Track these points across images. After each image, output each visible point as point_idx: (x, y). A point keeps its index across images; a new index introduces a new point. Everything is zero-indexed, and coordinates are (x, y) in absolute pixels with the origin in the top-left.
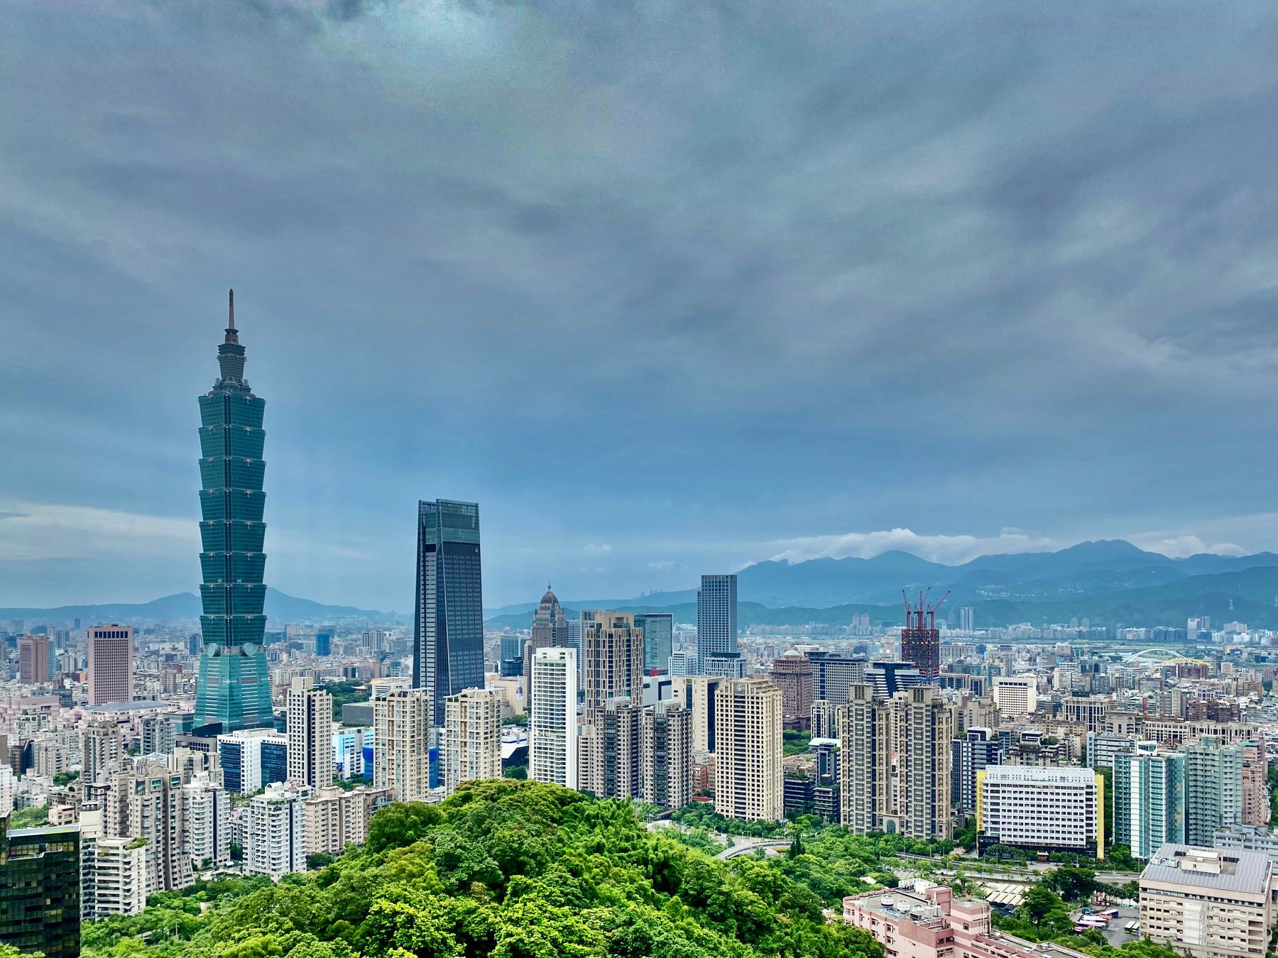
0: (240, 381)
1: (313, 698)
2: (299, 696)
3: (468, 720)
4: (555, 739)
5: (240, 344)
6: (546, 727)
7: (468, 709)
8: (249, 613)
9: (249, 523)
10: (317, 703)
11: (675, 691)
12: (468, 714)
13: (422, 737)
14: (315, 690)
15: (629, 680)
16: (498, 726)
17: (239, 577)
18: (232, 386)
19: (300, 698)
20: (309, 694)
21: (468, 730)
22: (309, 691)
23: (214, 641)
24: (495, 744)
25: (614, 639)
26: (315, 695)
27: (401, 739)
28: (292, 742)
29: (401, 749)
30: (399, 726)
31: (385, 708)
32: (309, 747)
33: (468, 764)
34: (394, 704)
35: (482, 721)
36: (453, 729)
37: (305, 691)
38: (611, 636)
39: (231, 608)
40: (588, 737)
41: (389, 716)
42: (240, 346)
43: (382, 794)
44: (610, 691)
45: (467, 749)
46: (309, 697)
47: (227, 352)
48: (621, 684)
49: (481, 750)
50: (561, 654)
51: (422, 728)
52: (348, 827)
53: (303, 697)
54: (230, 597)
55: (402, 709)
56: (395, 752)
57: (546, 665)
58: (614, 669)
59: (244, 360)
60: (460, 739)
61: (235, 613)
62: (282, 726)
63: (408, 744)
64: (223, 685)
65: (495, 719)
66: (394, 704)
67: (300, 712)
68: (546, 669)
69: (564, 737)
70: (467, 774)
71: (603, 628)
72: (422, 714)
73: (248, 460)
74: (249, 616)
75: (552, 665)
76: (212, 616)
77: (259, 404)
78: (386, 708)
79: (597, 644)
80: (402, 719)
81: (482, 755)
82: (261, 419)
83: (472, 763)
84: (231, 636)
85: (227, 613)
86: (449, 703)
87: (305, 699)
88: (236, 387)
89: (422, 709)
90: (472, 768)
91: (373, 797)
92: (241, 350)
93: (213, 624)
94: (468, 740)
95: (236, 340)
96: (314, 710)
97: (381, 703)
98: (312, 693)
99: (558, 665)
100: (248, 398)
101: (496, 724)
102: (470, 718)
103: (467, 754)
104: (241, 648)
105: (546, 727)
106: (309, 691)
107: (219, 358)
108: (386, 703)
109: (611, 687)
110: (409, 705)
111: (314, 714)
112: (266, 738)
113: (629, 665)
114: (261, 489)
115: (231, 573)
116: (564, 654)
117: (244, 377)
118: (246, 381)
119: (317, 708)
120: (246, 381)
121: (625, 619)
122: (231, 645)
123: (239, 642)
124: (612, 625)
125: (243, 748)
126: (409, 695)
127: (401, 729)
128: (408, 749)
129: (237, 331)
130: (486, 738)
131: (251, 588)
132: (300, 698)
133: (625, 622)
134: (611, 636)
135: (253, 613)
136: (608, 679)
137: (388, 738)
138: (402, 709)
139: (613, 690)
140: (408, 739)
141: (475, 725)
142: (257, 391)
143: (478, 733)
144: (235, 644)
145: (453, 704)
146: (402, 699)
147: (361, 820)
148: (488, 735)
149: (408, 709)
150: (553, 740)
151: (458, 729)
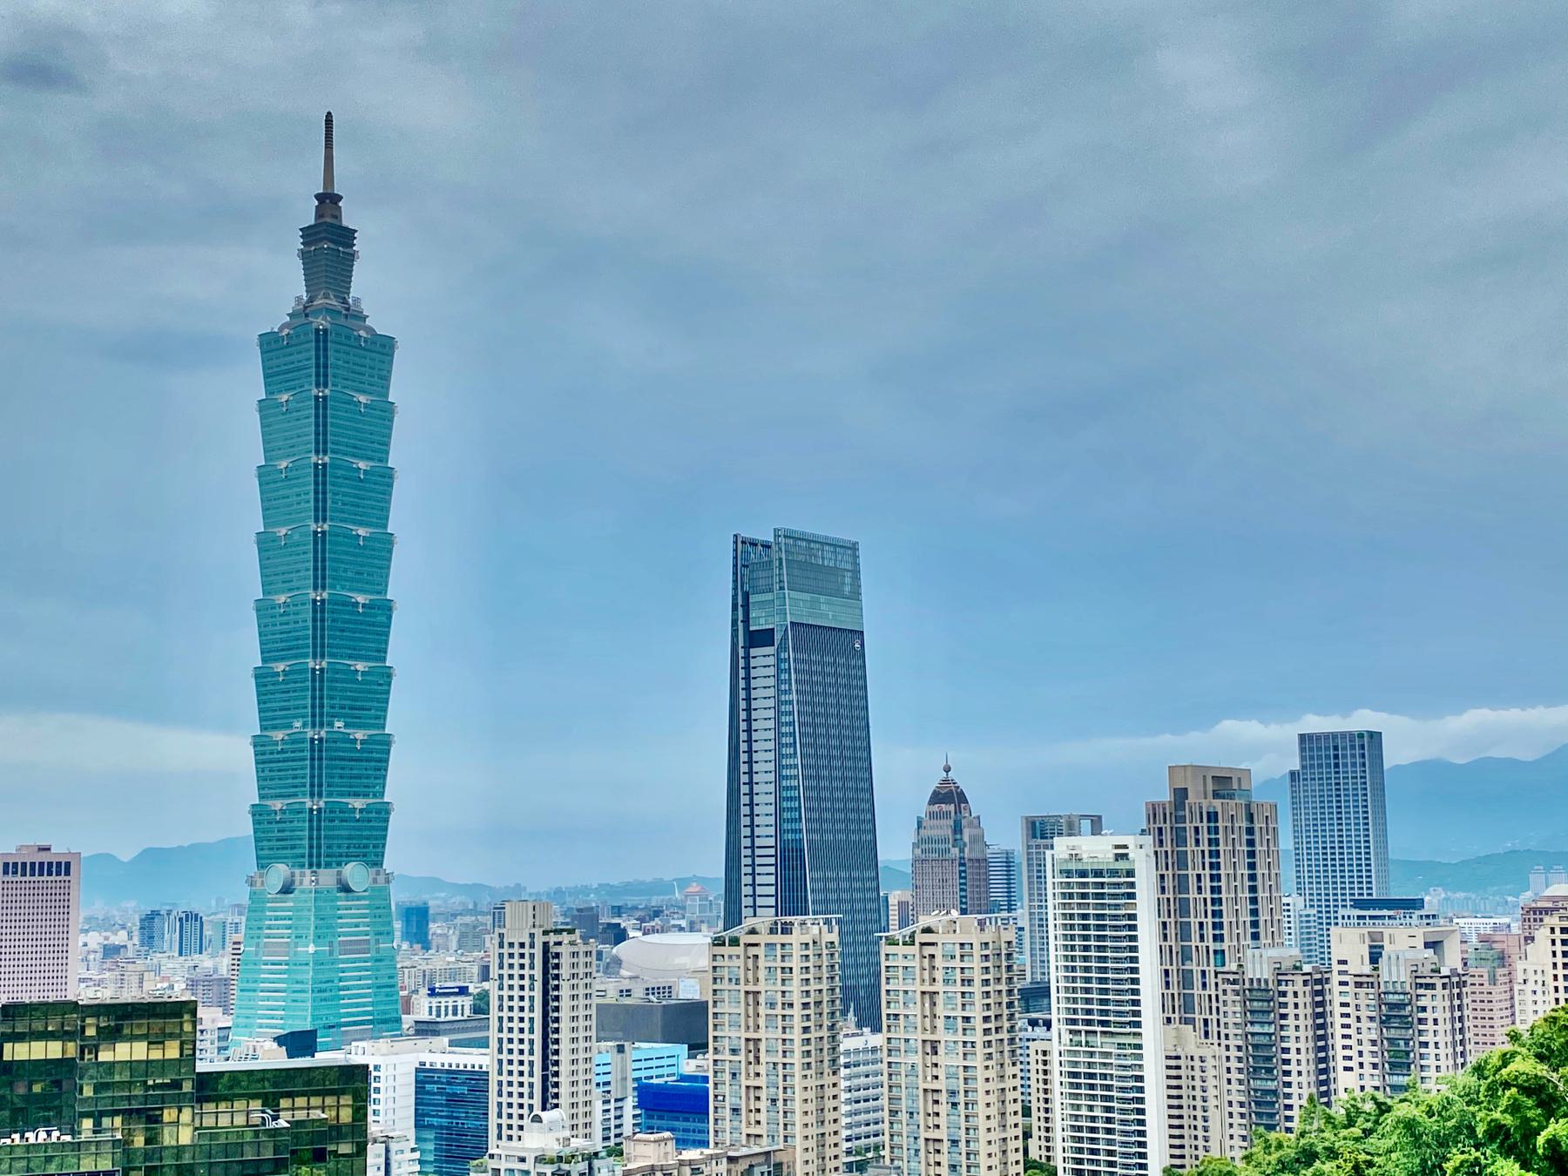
0: (345, 301)
2: (522, 945)
3: (939, 987)
5: (345, 223)
6: (1089, 1022)
7: (939, 962)
8: (356, 795)
10: (565, 961)
12: (939, 975)
13: (825, 1033)
14: (558, 932)
16: (1010, 1005)
18: (330, 311)
19: (526, 951)
20: (546, 939)
21: (941, 1011)
22: (546, 933)
23: (278, 858)
25: (1220, 824)
26: (559, 943)
28: (505, 1057)
29: (779, 1059)
30: (772, 1005)
31: (736, 962)
32: (545, 1068)
33: (943, 1097)
34: (761, 951)
35: (977, 988)
36: (901, 1011)
37: (538, 932)
38: (1212, 817)
39: (320, 785)
40: (1179, 1052)
42: (346, 229)
43: (762, 1159)
44: (1218, 946)
45: (941, 1059)
46: (546, 944)
47: (321, 240)
48: (1241, 931)
49: (978, 1061)
50: (1117, 847)
53: (532, 946)
55: (779, 964)
56: (762, 1069)
57: (1083, 874)
59: (352, 257)
61: (330, 795)
62: (470, 1031)
63: (798, 1047)
64: (302, 959)
65: (1003, 987)
66: (761, 951)
67: (526, 982)
68: (1085, 885)
69: (1139, 1047)
70: (942, 1121)
71: (1192, 799)
74: (358, 803)
75: (1098, 873)
76: (278, 804)
78: (740, 963)
80: (780, 987)
81: (980, 1074)
82: (386, 378)
83: (953, 1093)
84: (319, 847)
85: (312, 795)
86: (892, 949)
89: (825, 964)
90: (954, 1105)
92: (347, 236)
94: (941, 1035)
95: (338, 217)
96: (557, 977)
97: (727, 950)
98: (553, 938)
99: (1114, 873)
100: (362, 333)
101: (1005, 1000)
102: (946, 982)
103: (941, 1073)
104: (339, 873)
105: (1089, 1022)
106: (546, 933)
107: (304, 255)
108: (740, 950)
109: (1218, 938)
110: (797, 952)
111: (557, 988)
112: (428, 1058)
116: (1125, 847)
117: (354, 292)
118: (357, 300)
119: (565, 972)
120: (357, 300)
121: (1235, 782)
122: (319, 866)
123: (337, 860)
124: (1210, 794)
126: (796, 929)
127: (779, 1011)
128: (796, 1059)
130: (987, 1031)
131: (363, 742)
132: (526, 951)
133: (1235, 786)
134: (1212, 817)
135: (366, 795)
136: (1210, 920)
137: (745, 1035)
138: (779, 964)
139: (1225, 946)
140: (796, 1035)
141: (959, 1000)
142: (379, 321)
143: (967, 1019)
144: (328, 865)
145: (901, 950)
146: (779, 938)
148: (992, 1025)
149: (795, 963)
150: (1108, 1055)
151: (914, 1010)
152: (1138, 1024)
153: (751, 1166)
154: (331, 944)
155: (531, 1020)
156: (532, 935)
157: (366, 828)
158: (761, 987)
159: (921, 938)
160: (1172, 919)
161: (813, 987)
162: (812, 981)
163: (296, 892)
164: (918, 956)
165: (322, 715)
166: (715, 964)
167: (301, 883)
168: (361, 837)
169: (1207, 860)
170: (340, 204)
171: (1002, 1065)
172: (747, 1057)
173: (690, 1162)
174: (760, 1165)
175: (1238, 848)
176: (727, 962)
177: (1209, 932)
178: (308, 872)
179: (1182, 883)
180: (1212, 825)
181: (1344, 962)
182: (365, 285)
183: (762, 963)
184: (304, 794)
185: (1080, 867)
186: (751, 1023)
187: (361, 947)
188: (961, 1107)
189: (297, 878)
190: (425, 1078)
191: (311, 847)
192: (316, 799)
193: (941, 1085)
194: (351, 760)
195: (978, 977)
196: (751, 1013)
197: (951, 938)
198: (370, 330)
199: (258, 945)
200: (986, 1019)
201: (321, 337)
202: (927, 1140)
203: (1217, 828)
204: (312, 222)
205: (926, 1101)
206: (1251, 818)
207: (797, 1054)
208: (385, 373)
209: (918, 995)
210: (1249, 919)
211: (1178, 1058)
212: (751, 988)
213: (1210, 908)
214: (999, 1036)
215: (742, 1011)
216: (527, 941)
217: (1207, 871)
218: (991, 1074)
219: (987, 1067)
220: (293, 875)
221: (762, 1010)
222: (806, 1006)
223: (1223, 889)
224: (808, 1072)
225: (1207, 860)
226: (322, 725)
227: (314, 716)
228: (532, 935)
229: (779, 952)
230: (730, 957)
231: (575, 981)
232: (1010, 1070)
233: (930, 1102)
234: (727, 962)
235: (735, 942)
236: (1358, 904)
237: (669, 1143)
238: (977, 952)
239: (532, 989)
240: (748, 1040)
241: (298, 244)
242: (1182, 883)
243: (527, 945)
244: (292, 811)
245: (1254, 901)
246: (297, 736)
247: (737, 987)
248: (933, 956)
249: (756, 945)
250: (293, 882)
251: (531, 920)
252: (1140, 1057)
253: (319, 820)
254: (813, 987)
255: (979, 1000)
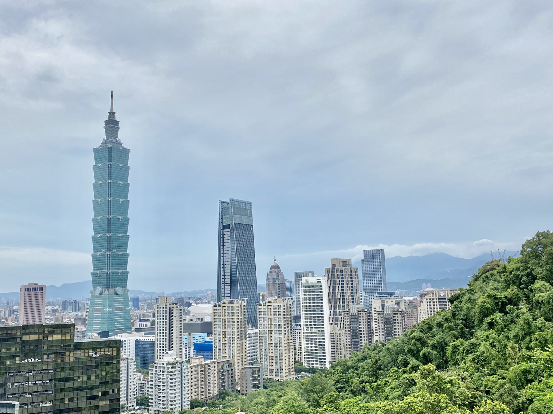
0: (116, 140)
1: (172, 309)
2: (163, 308)
3: (272, 316)
4: (317, 332)
5: (116, 120)
6: (311, 325)
7: (272, 310)
8: (119, 269)
9: (120, 218)
10: (175, 312)
11: (374, 308)
12: (272, 313)
13: (243, 329)
15: (353, 299)
16: (291, 321)
17: (115, 248)
18: (112, 142)
19: (164, 309)
20: (170, 306)
21: (273, 323)
22: (170, 304)
24: (290, 332)
25: (344, 273)
26: (173, 307)
27: (231, 330)
28: (159, 337)
29: (231, 336)
30: (229, 322)
31: (220, 311)
32: (169, 340)
33: (273, 345)
34: (226, 308)
35: (282, 317)
36: (263, 323)
37: (167, 304)
38: (342, 271)
39: (110, 266)
40: (334, 332)
41: (223, 316)
42: (117, 121)
43: (227, 362)
44: (344, 305)
45: (273, 335)
46: (170, 307)
47: (110, 124)
49: (282, 336)
50: (318, 280)
51: (243, 323)
52: (209, 383)
53: (166, 308)
54: (110, 260)
56: (227, 339)
57: (309, 287)
58: (345, 292)
59: (118, 128)
60: (268, 329)
61: (112, 269)
62: (150, 330)
63: (236, 333)
65: (289, 316)
66: (226, 308)
67: (164, 318)
68: (310, 289)
69: (324, 331)
70: (273, 351)
71: (337, 267)
72: (243, 314)
73: (121, 182)
74: (120, 271)
75: (313, 286)
76: (98, 272)
77: (126, 152)
78: (221, 311)
79: (334, 277)
81: (283, 339)
82: (127, 160)
83: (276, 344)
85: (107, 269)
87: (168, 309)
88: (115, 143)
89: (243, 311)
90: (276, 347)
91: (222, 364)
92: (117, 122)
93: (99, 276)
94: (273, 329)
95: (114, 118)
96: (173, 316)
97: (217, 308)
98: (171, 306)
99: (317, 286)
100: (121, 148)
101: (289, 320)
102: (274, 315)
103: (273, 339)
104: (115, 290)
106: (170, 304)
107: (105, 128)
108: (221, 308)
110: (236, 308)
111: (173, 319)
112: (138, 338)
113: (352, 290)
114: (127, 198)
115: (110, 246)
116: (320, 279)
118: (119, 140)
119: (175, 315)
121: (347, 262)
122: (109, 288)
123: (115, 286)
125: (125, 343)
126: (235, 302)
127: (231, 324)
128: (236, 336)
129: (115, 113)
130: (285, 328)
131: (121, 255)
132: (164, 309)
134: (342, 271)
135: (122, 269)
136: (341, 298)
139: (345, 304)
140: (235, 330)
141: (278, 320)
143: (279, 325)
144: (112, 288)
145: (262, 307)
146: (231, 305)
147: (216, 378)
148: (286, 326)
149: (235, 311)
150: (316, 333)
151: (266, 323)
152: (323, 325)
153: (224, 364)
154: (112, 308)
155: (166, 327)
156: (166, 305)
157: (122, 278)
158: (226, 317)
159: (268, 304)
160: (332, 298)
161: (240, 317)
162: (239, 316)
163: (103, 295)
164: (267, 309)
165: (110, 248)
166: (214, 312)
167: (105, 292)
168: (120, 280)
169: (341, 283)
170: (115, 114)
171: (289, 336)
172: (223, 336)
173: (208, 364)
174: (225, 364)
175: (348, 279)
176: (217, 311)
177: (341, 301)
178: (106, 289)
179: (334, 289)
180: (342, 273)
181: (375, 308)
182: (121, 136)
183: (226, 311)
184: (105, 269)
185: (308, 285)
186: (224, 327)
187: (120, 309)
188: (278, 347)
189: (104, 291)
190: (137, 342)
191: (107, 283)
192: (108, 270)
193: (273, 342)
194: (118, 260)
195: (282, 314)
196: (224, 324)
197: (275, 304)
198: (123, 147)
199: (93, 309)
200: (285, 325)
201: (110, 149)
202: (269, 356)
203: (343, 274)
204: (108, 119)
205: (269, 346)
206: (351, 272)
207: (236, 335)
208: (127, 158)
209: (267, 319)
210: (351, 298)
211: (333, 333)
212: (224, 318)
213: (341, 295)
214: (288, 329)
215: (221, 324)
216: (165, 307)
217: (341, 285)
218: (286, 339)
219: (285, 337)
220: (102, 290)
221: (227, 323)
222: (238, 322)
223: (345, 290)
224: (238, 339)
225: (341, 283)
226: (110, 251)
227: (108, 248)
228: (166, 305)
229: (231, 308)
230: (218, 310)
231: (177, 317)
232: (291, 338)
233: (270, 346)
234: (217, 311)
235: (219, 306)
236: (379, 293)
237: (202, 359)
238: (282, 307)
239: (166, 319)
240: (223, 331)
241: (104, 125)
242: (334, 289)
243: (165, 308)
244: (102, 274)
245: (352, 293)
246: (103, 254)
247: (220, 318)
248: (271, 309)
249: (225, 307)
250: (102, 292)
251: (166, 302)
252: (324, 333)
253: (109, 276)
254: (240, 317)
255: (282, 320)
